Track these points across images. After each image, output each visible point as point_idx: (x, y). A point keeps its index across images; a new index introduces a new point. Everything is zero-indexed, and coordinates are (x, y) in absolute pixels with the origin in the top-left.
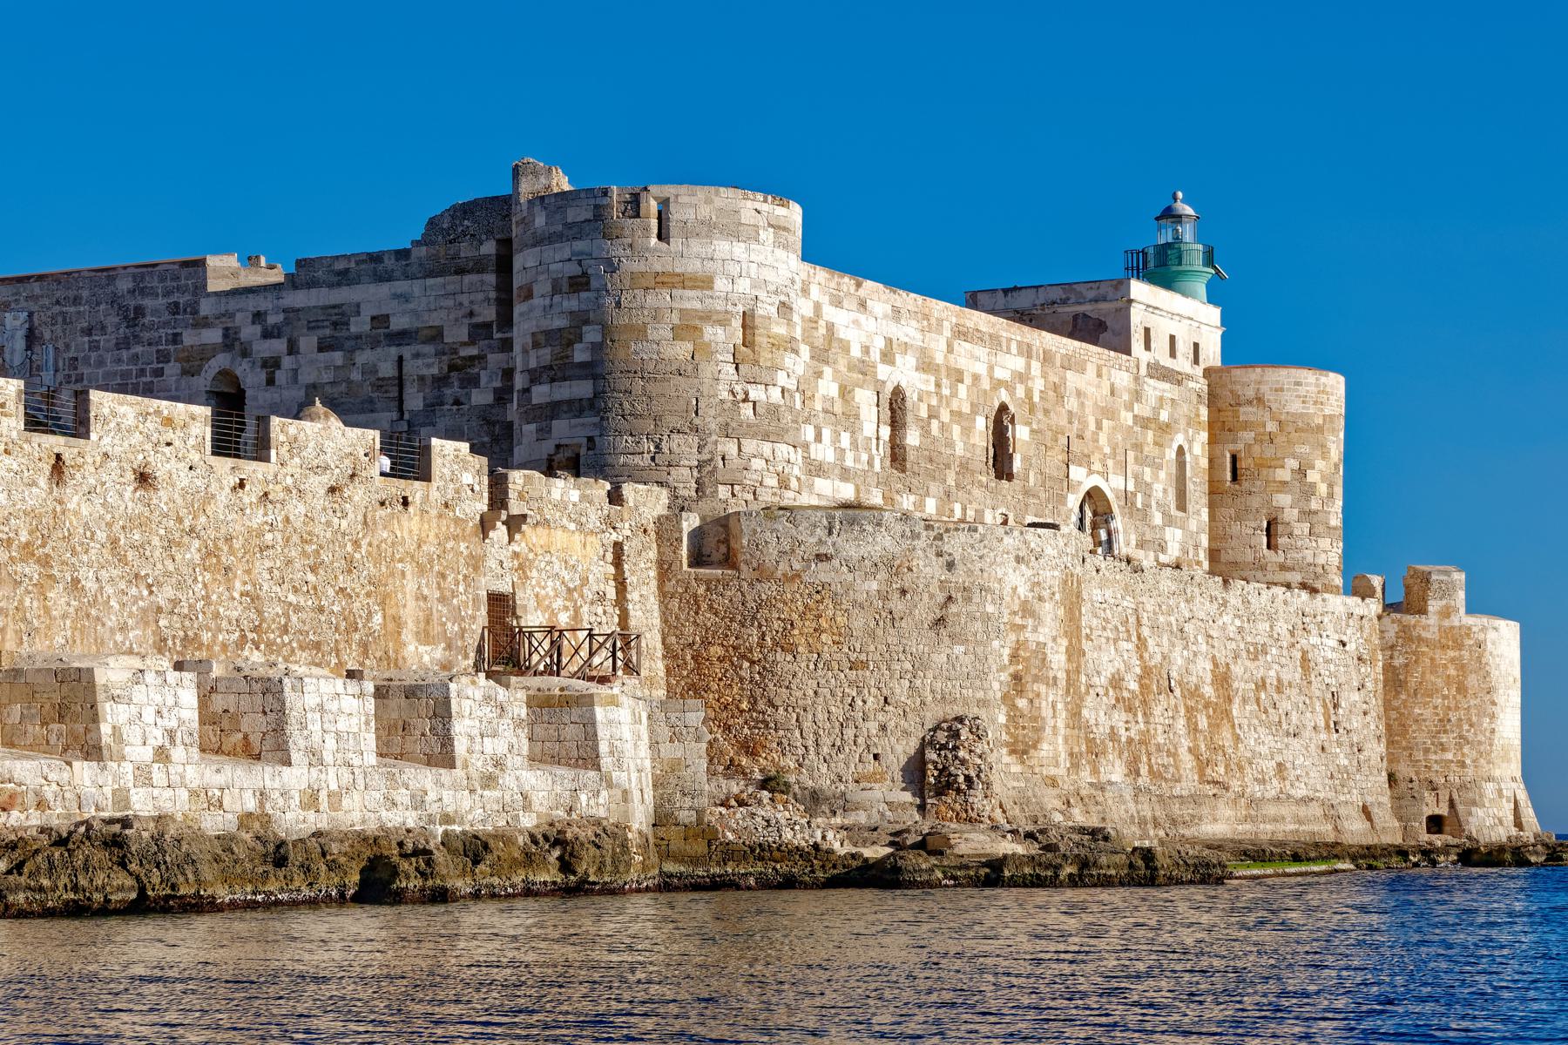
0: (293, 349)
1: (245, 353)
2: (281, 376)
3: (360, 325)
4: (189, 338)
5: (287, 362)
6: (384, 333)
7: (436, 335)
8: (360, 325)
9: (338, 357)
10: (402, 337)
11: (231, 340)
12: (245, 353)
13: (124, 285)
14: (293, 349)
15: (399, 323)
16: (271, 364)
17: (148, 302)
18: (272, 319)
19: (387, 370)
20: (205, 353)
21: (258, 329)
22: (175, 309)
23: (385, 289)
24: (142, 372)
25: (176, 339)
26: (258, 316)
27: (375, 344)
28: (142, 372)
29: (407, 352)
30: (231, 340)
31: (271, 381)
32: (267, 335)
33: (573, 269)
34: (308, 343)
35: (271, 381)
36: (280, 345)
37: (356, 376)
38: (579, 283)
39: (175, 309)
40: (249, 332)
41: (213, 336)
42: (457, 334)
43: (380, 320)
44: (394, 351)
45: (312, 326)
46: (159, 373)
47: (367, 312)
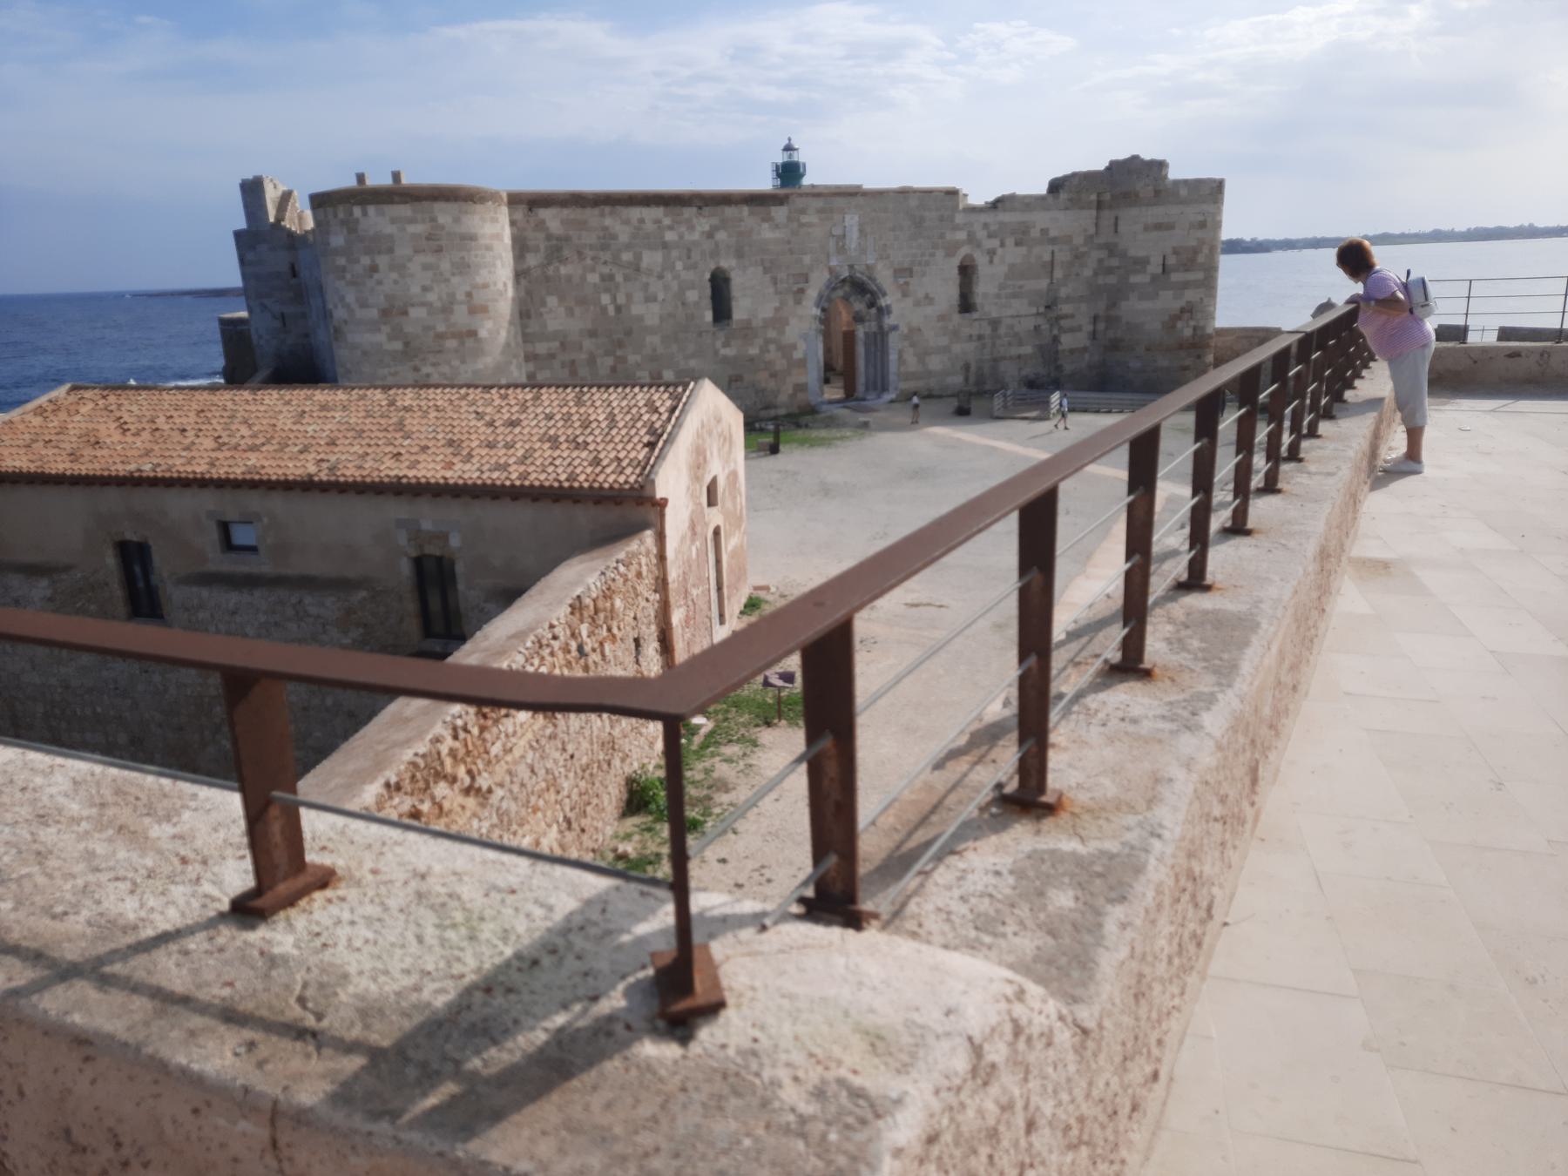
0: (1002, 245)
1: (979, 245)
2: (996, 260)
3: (1035, 233)
4: (949, 236)
5: (1000, 251)
6: (1047, 238)
7: (1068, 239)
8: (1035, 233)
9: (1023, 250)
10: (1053, 241)
11: (971, 238)
13: (913, 202)
14: (1002, 245)
15: (1053, 233)
16: (992, 253)
18: (993, 228)
19: (1047, 257)
20: (956, 246)
21: (985, 233)
24: (923, 255)
25: (942, 236)
26: (986, 226)
28: (923, 255)
29: (1056, 248)
30: (971, 238)
31: (991, 262)
32: (990, 236)
33: (1201, 218)
34: (1010, 241)
35: (991, 262)
36: (995, 243)
39: (941, 219)
40: (981, 234)
41: (961, 235)
42: (1079, 240)
43: (1044, 231)
44: (1050, 248)
46: (932, 255)
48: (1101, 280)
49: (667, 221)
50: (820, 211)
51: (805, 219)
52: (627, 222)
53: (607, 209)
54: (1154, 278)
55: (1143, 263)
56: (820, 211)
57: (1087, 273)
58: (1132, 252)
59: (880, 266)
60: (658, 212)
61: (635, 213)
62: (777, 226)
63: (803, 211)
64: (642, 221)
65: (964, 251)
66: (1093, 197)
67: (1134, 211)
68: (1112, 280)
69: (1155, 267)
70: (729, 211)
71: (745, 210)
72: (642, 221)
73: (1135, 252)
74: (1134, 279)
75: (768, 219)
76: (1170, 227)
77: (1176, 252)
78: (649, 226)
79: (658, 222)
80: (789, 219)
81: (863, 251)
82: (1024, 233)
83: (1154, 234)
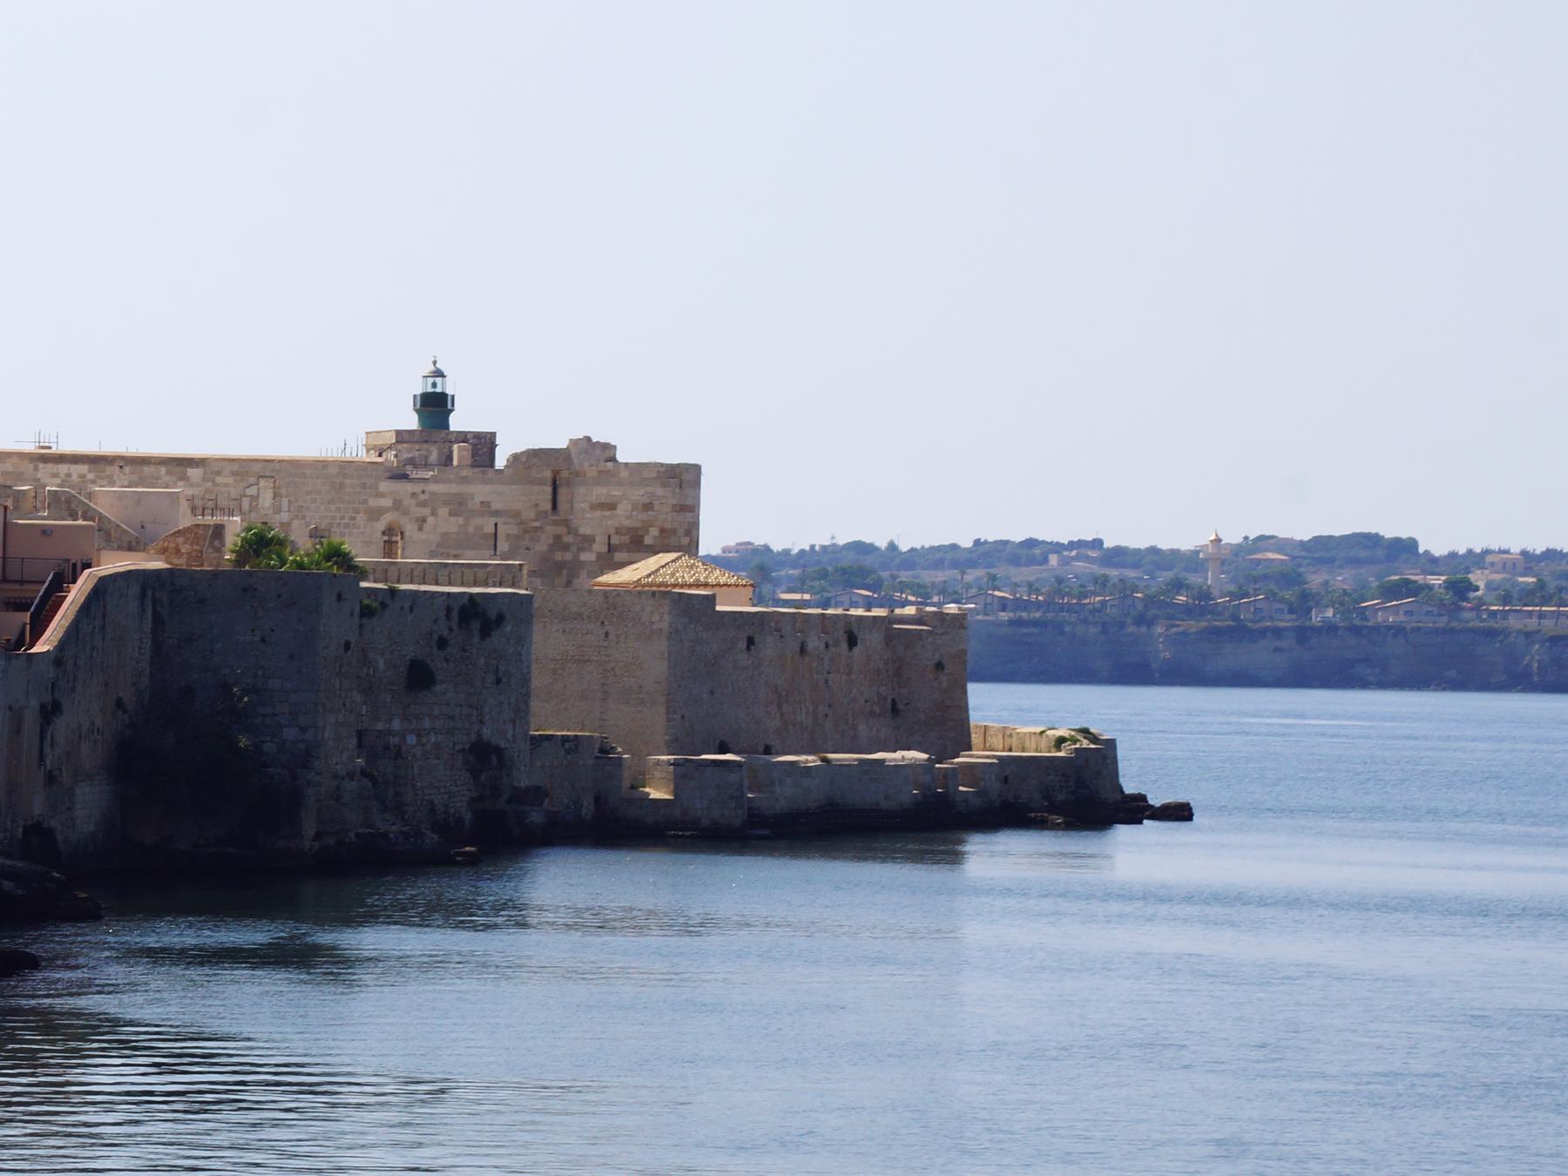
0: (434, 513)
1: (406, 513)
2: (427, 526)
4: (373, 503)
5: (430, 520)
7: (516, 515)
9: (461, 520)
10: (497, 513)
12: (406, 513)
15: (495, 506)
17: (348, 482)
19: (490, 529)
20: (381, 511)
22: (364, 486)
23: (488, 488)
24: (343, 518)
25: (365, 502)
26: (414, 495)
27: (482, 514)
28: (343, 518)
29: (500, 521)
30: (397, 505)
31: (420, 529)
34: (443, 512)
35: (420, 529)
36: (426, 511)
37: (471, 530)
38: (648, 507)
40: (408, 502)
41: (387, 502)
42: (529, 514)
44: (493, 520)
45: (446, 503)
47: (478, 499)
48: (558, 556)
49: (90, 476)
50: (234, 474)
51: (219, 480)
52: (56, 475)
53: (41, 465)
54: (599, 556)
55: (589, 540)
56: (234, 474)
57: (541, 547)
58: (582, 531)
59: (295, 524)
60: (83, 469)
61: (63, 468)
62: (192, 485)
63: (218, 473)
64: (69, 475)
65: (388, 518)
66: (548, 474)
67: (582, 490)
68: (568, 556)
69: (600, 546)
70: (147, 470)
71: (163, 470)
72: (69, 475)
73: (585, 530)
74: (584, 557)
75: (184, 478)
76: (612, 507)
77: (618, 532)
78: (74, 477)
79: (83, 476)
80: (204, 479)
81: (278, 510)
82: (460, 504)
83: (597, 514)
